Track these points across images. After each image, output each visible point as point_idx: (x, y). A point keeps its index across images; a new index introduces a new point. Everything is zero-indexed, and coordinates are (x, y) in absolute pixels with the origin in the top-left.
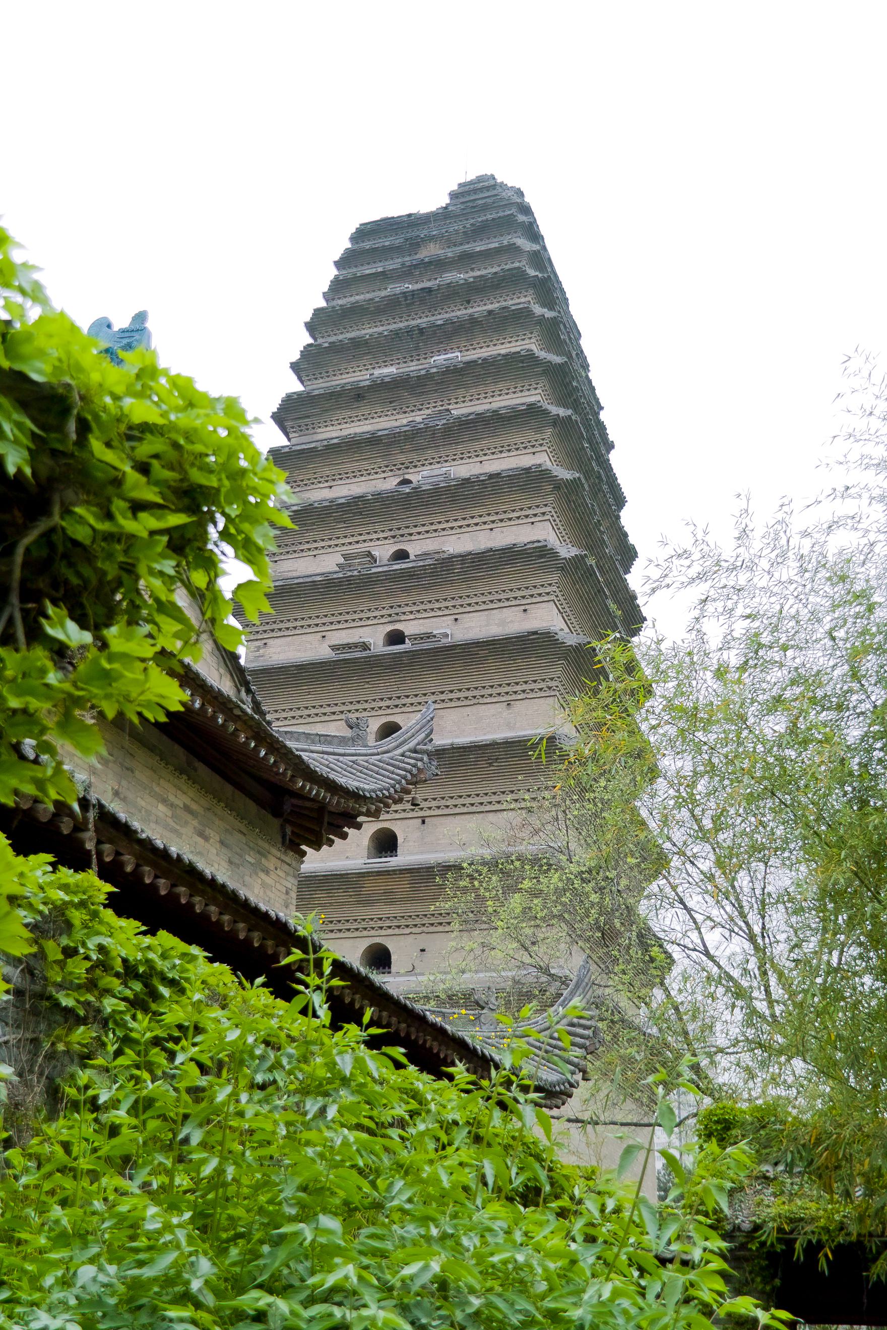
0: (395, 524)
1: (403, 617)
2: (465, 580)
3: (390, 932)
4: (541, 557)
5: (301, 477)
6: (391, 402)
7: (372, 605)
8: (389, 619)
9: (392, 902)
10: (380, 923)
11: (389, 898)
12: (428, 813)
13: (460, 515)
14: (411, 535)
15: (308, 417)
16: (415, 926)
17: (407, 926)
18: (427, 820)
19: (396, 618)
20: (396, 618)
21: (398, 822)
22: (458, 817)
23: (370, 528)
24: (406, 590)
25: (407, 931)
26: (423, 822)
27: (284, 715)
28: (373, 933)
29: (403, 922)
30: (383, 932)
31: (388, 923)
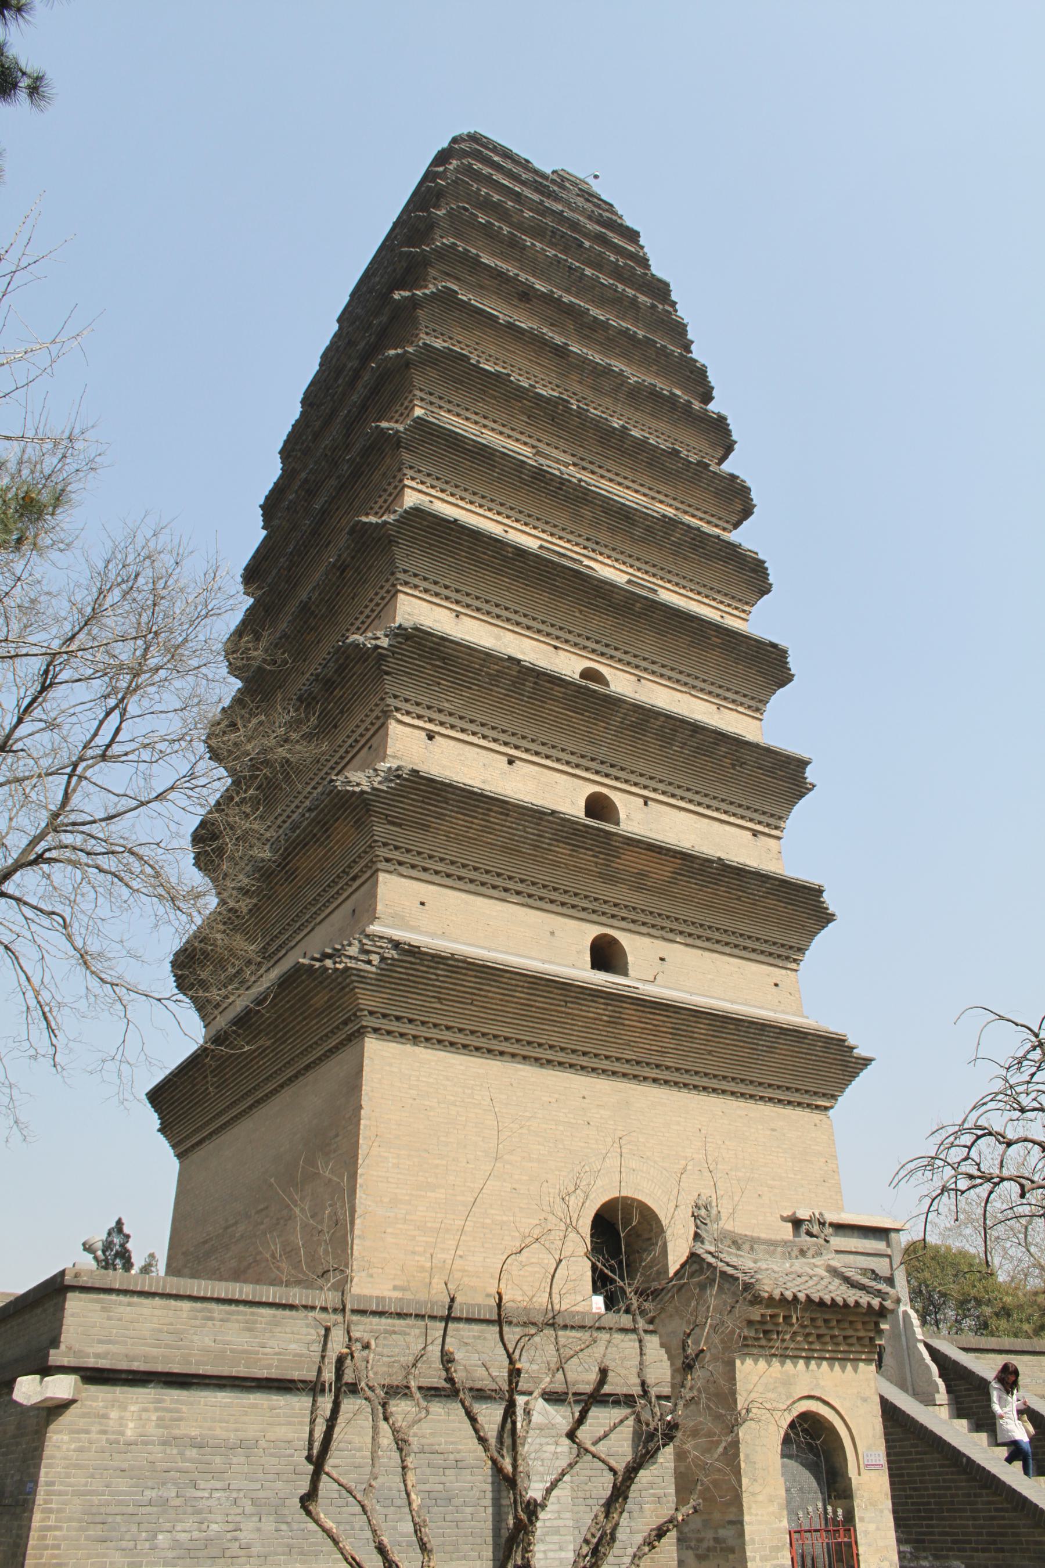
0: (581, 452)
2: (675, 554)
3: (623, 924)
4: (754, 571)
5: (460, 338)
6: (552, 325)
9: (639, 889)
10: (615, 911)
11: (639, 882)
12: (652, 795)
13: (649, 482)
16: (653, 926)
17: (644, 924)
18: (649, 803)
21: (619, 794)
23: (554, 440)
24: (611, 529)
28: (603, 919)
29: (642, 917)
31: (624, 913)
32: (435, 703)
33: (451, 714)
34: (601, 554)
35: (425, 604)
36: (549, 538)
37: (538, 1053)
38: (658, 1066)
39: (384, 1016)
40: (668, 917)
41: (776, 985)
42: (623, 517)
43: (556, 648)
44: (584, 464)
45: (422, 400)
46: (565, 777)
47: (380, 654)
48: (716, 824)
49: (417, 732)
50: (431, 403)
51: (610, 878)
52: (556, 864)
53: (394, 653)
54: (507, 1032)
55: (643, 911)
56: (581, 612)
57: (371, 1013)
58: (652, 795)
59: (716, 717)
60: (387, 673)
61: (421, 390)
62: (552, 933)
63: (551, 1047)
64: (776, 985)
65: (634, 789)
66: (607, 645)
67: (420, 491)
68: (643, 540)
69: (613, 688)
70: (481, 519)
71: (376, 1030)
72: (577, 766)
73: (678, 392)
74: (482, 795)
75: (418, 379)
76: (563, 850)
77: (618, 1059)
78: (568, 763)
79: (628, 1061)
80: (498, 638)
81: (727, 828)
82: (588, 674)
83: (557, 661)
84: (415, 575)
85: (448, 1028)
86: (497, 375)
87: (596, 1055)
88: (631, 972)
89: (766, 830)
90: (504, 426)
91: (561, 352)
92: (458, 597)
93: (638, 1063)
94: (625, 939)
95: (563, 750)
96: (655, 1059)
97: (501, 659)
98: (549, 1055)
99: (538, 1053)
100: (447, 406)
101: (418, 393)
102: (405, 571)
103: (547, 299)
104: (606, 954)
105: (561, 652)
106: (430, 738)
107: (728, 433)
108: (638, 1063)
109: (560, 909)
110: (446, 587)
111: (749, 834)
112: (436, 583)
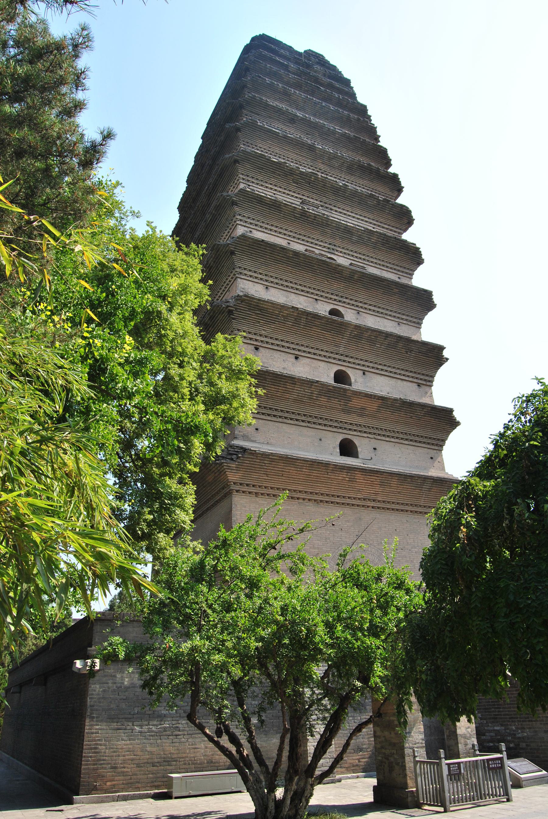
0: (325, 200)
1: (336, 253)
3: (355, 433)
5: (261, 146)
6: (307, 134)
7: (321, 238)
8: (327, 250)
9: (361, 415)
12: (367, 369)
13: (359, 212)
14: (331, 209)
15: (258, 115)
16: (370, 433)
17: (365, 432)
18: (366, 373)
19: (332, 251)
20: (332, 251)
21: (350, 369)
22: (383, 377)
23: (311, 195)
25: (365, 435)
26: (364, 374)
27: (272, 280)
28: (345, 431)
29: (364, 429)
30: (351, 433)
31: (355, 428)
32: (258, 332)
33: (266, 337)
34: (337, 251)
35: (251, 283)
36: (311, 245)
37: (315, 497)
38: (374, 501)
39: (241, 484)
40: (377, 428)
41: (432, 458)
42: (347, 232)
43: (316, 300)
44: (327, 205)
45: (243, 179)
46: (323, 363)
47: (229, 310)
48: (399, 381)
49: (250, 346)
50: (248, 181)
51: (347, 411)
52: (320, 406)
53: (236, 309)
54: (300, 488)
55: (364, 426)
56: (328, 281)
57: (234, 483)
58: (367, 369)
59: (398, 328)
60: (234, 319)
61: (243, 174)
62: (320, 440)
63: (322, 494)
64: (432, 458)
65: (358, 367)
66: (342, 297)
67: (245, 226)
68: (357, 242)
69: (346, 319)
70: (276, 238)
71: (237, 491)
72: (329, 357)
73: (373, 164)
74: (282, 375)
75: (240, 169)
76: (323, 400)
77: (354, 498)
78: (325, 356)
79: (359, 499)
80: (287, 297)
81: (405, 383)
82: (333, 312)
83: (317, 306)
84: (245, 269)
85: (272, 488)
86: (279, 163)
87: (344, 497)
88: (360, 456)
89: (424, 383)
90: (285, 189)
91: (311, 148)
92: (267, 278)
93: (364, 499)
94: (357, 441)
95: (322, 350)
96: (373, 497)
97: (289, 308)
98: (321, 498)
99: (315, 497)
100: (256, 181)
101: (241, 176)
102: (240, 267)
103: (303, 120)
104: (347, 448)
105: (319, 302)
106: (257, 349)
107: (399, 183)
108: (364, 499)
109: (323, 428)
110: (261, 274)
111: (415, 386)
112: (255, 272)
